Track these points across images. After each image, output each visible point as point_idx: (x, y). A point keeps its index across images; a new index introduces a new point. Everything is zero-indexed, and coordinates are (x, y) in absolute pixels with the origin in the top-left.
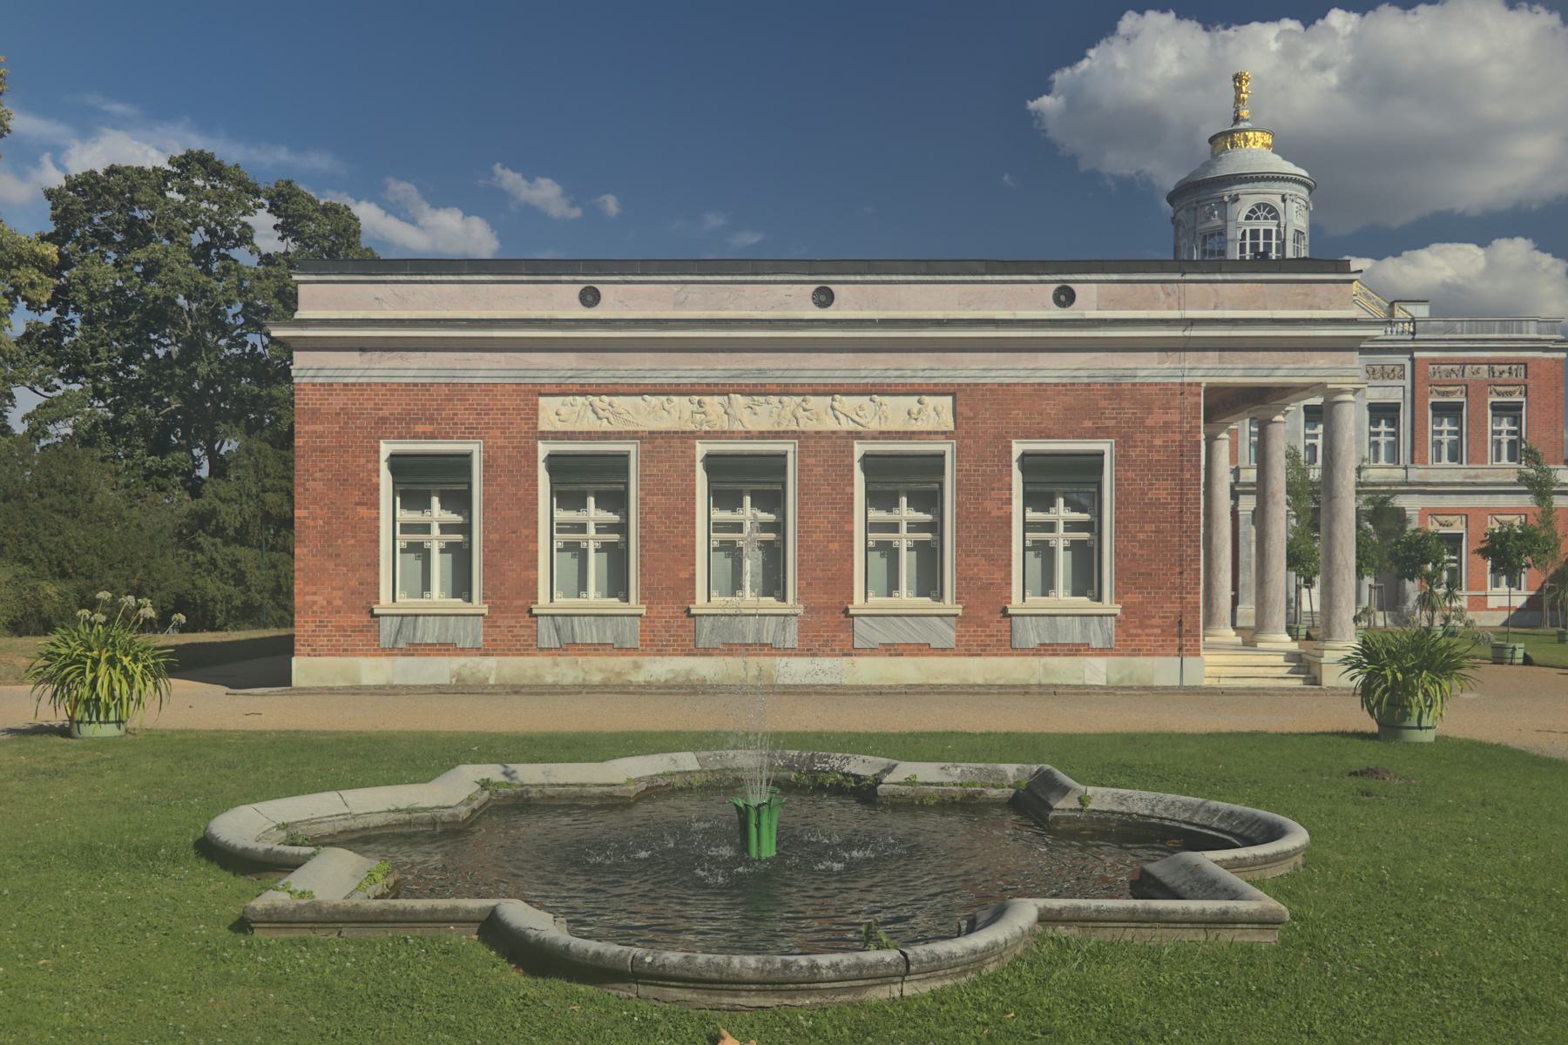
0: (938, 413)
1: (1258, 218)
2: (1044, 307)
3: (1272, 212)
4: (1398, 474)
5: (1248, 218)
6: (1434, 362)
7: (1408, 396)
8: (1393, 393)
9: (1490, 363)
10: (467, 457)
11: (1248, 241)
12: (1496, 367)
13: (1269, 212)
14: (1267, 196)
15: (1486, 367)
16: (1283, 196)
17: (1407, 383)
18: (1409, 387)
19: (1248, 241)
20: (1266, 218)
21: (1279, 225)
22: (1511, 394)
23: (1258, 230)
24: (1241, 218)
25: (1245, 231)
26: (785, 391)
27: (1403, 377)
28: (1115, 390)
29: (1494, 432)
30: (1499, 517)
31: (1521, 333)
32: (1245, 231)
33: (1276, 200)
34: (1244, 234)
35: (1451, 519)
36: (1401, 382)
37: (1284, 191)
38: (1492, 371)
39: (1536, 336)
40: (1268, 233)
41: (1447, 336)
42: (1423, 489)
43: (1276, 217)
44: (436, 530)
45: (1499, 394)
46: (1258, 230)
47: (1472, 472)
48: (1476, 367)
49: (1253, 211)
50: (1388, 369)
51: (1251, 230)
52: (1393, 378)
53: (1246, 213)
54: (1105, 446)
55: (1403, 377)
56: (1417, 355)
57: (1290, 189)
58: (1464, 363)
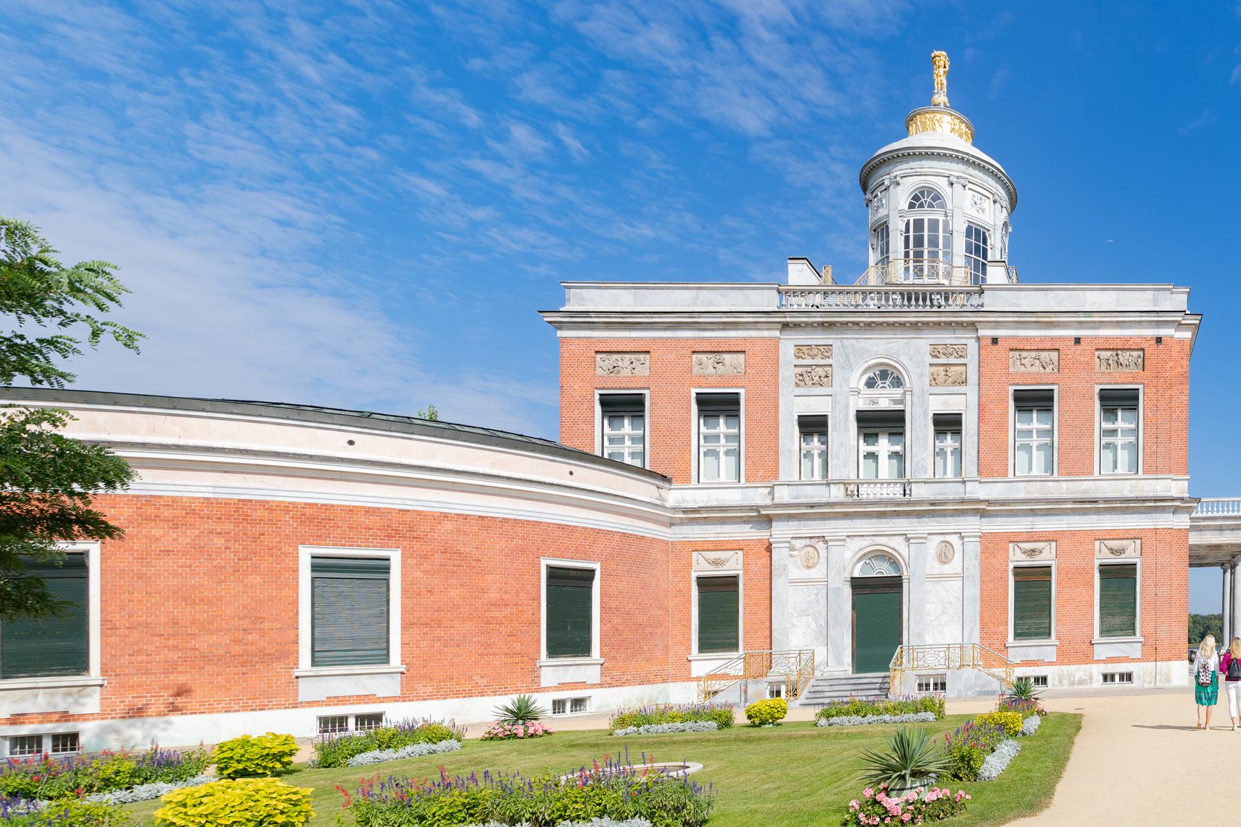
1: (921, 206)
5: (911, 206)
13: (934, 199)
19: (911, 234)
20: (931, 206)
21: (946, 215)
23: (923, 219)
24: (904, 205)
25: (909, 221)
32: (909, 221)
33: (941, 184)
34: (908, 224)
37: (950, 173)
40: (934, 224)
43: (943, 206)
46: (923, 219)
49: (916, 198)
51: (914, 220)
53: (910, 200)
57: (956, 169)
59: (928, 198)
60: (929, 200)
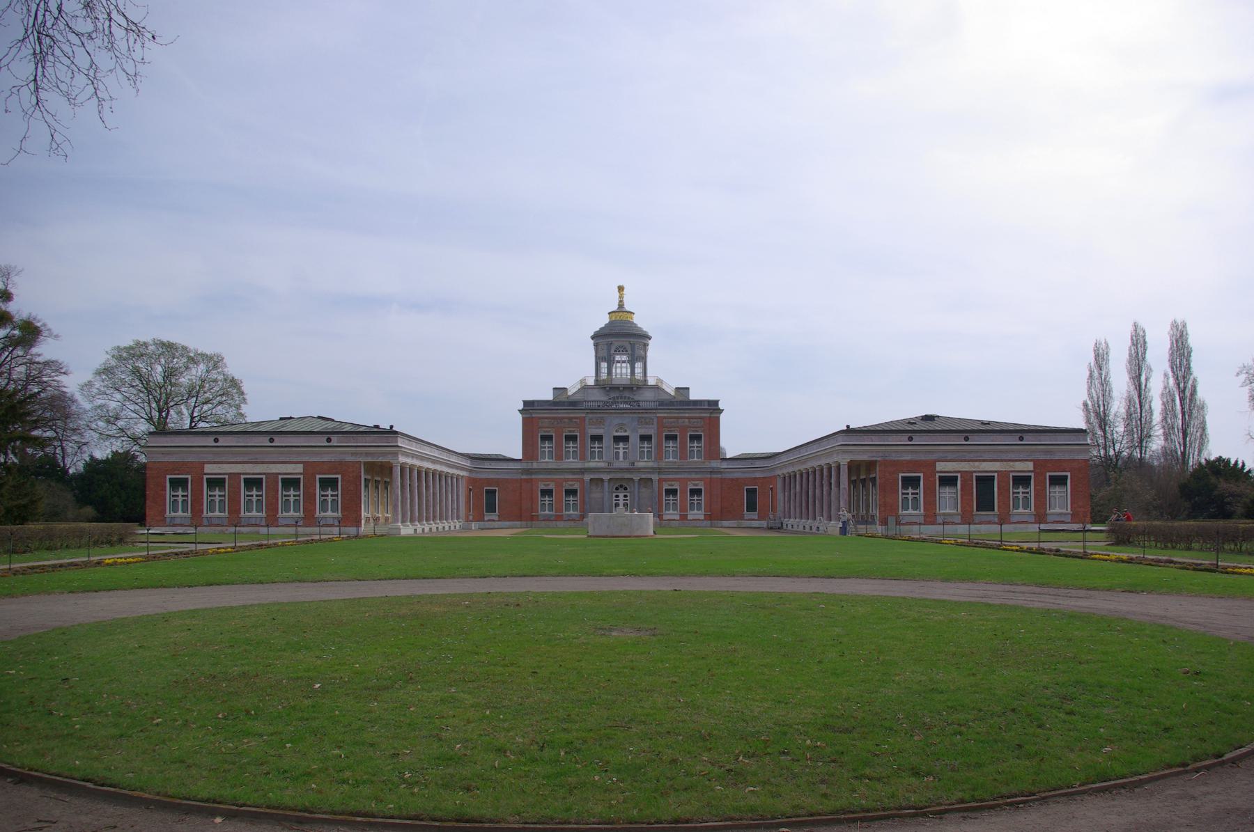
0: (299, 468)
1: (619, 351)
2: (324, 442)
4: (650, 464)
6: (665, 418)
7: (656, 432)
8: (650, 431)
9: (689, 418)
10: (187, 479)
15: (687, 420)
17: (655, 426)
18: (656, 428)
22: (697, 431)
26: (263, 463)
28: (341, 463)
29: (690, 447)
30: (693, 482)
35: (673, 483)
36: (653, 426)
38: (689, 422)
39: (707, 407)
41: (671, 407)
42: (659, 471)
44: (217, 496)
45: (693, 431)
47: (681, 464)
49: (617, 348)
50: (647, 420)
54: (339, 477)
55: (653, 424)
58: (678, 418)
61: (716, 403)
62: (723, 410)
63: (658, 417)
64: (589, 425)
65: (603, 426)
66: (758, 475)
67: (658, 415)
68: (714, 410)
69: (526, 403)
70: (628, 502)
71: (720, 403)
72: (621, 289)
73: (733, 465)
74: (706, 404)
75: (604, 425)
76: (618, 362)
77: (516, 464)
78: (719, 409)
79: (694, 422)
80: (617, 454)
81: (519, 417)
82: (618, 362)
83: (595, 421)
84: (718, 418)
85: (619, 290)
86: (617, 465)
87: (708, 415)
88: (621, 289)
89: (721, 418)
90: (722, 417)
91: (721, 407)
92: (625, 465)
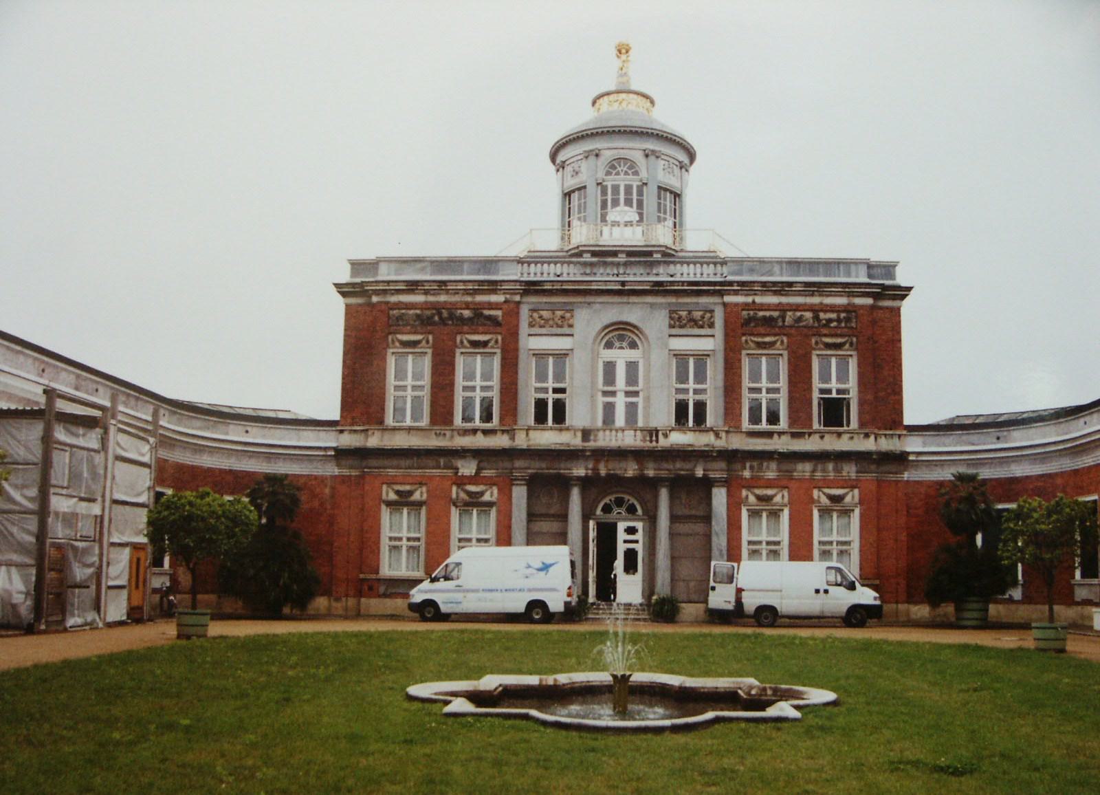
1: (618, 174)
3: (632, 167)
5: (608, 173)
11: (609, 197)
12: (822, 315)
13: (630, 168)
14: (625, 151)
15: (808, 315)
16: (645, 150)
20: (626, 173)
27: (711, 325)
31: (849, 275)
33: (638, 157)
38: (816, 318)
39: (866, 280)
48: (798, 314)
50: (697, 315)
52: (702, 327)
56: (727, 299)
59: (624, 166)
60: (625, 169)
61: (889, 269)
62: (909, 289)
63: (725, 305)
64: (531, 325)
65: (566, 330)
66: (1019, 470)
67: (727, 299)
68: (883, 287)
69: (357, 266)
70: (639, 548)
71: (898, 270)
72: (623, 50)
73: (938, 445)
74: (863, 270)
75: (571, 326)
76: (615, 224)
77: (322, 434)
78: (899, 288)
79: (830, 321)
80: (609, 409)
81: (338, 305)
82: (615, 224)
83: (545, 314)
84: (896, 312)
85: (620, 51)
86: (606, 440)
87: (869, 301)
88: (623, 50)
89: (902, 309)
90: (908, 308)
91: (902, 278)
92: (630, 440)
